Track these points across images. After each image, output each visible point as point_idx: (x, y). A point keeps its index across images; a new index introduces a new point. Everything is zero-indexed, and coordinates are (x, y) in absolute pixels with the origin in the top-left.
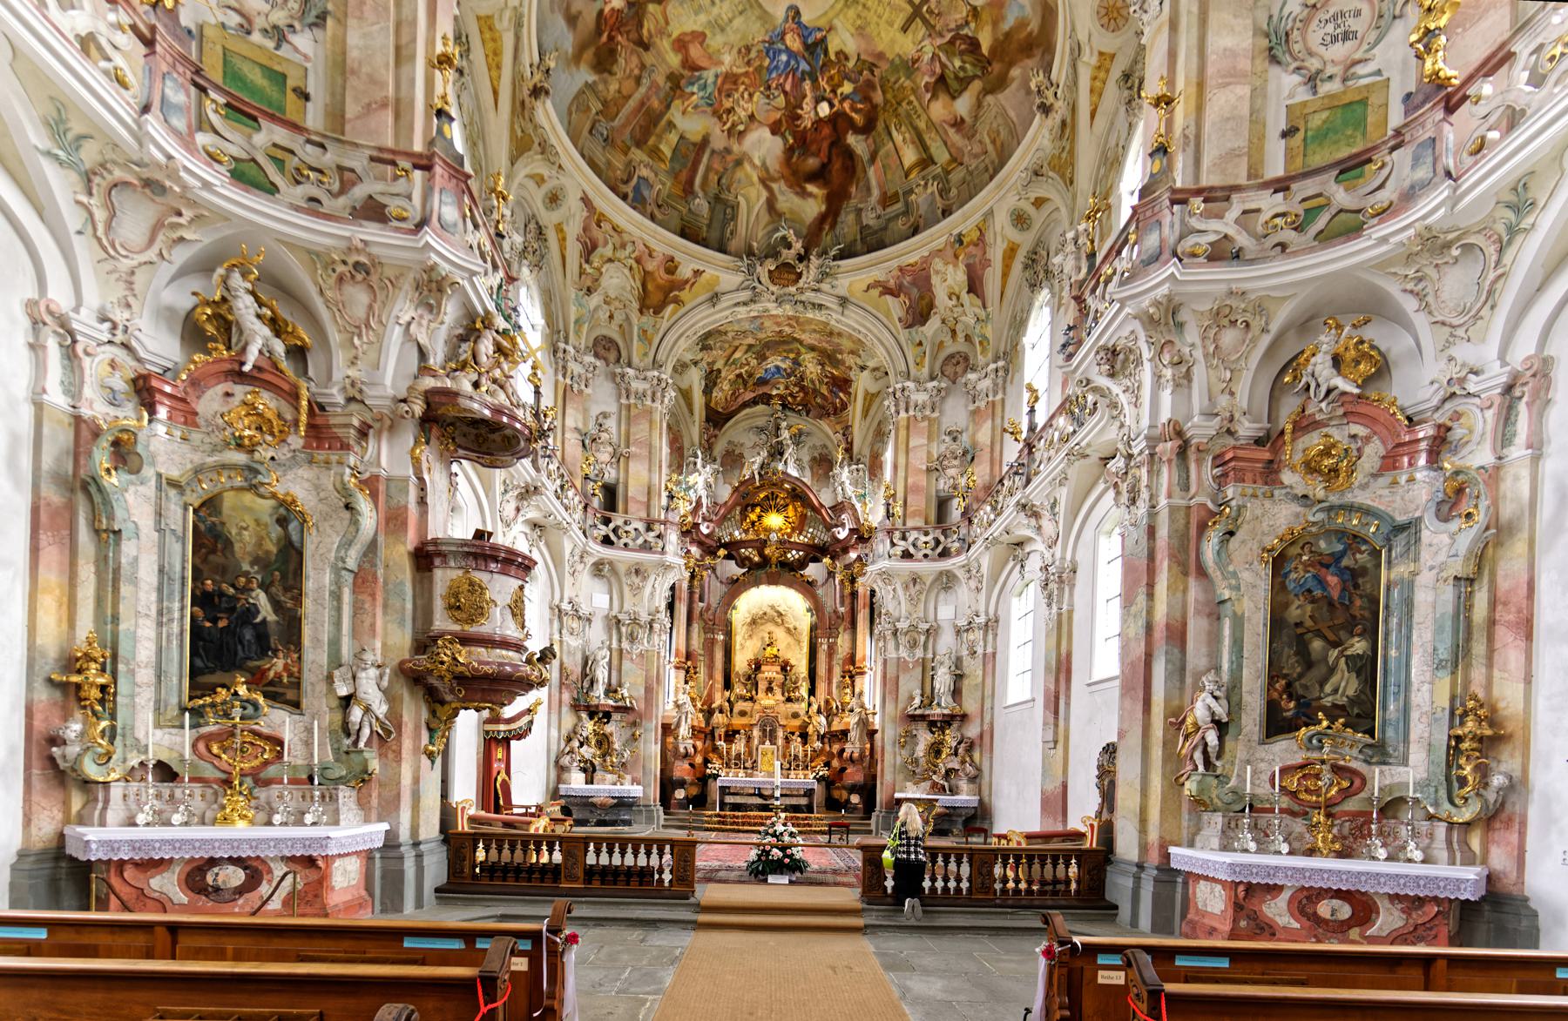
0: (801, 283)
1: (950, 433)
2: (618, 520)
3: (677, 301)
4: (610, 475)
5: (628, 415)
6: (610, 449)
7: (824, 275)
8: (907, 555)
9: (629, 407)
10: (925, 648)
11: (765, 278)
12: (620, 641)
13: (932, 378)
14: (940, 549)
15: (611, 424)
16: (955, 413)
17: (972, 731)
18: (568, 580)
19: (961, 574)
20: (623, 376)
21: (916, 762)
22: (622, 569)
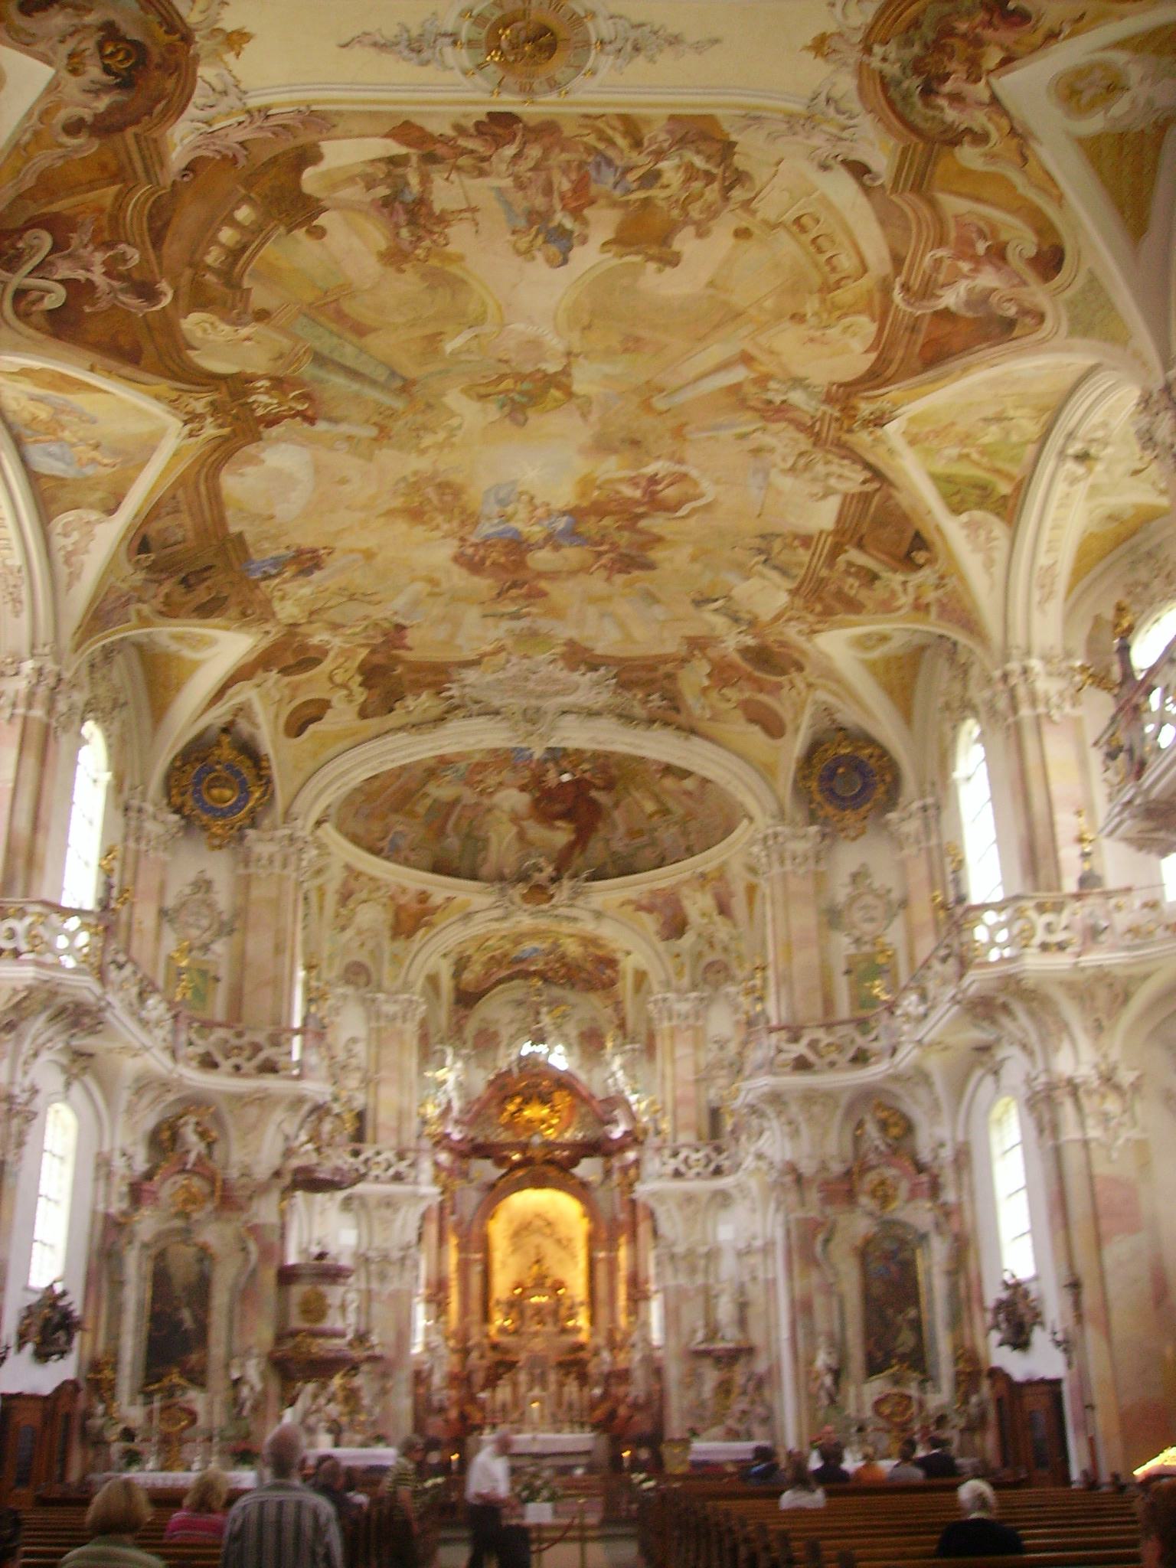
0: (554, 901)
1: (716, 1042)
2: (368, 1152)
3: (430, 925)
4: (360, 1101)
5: (378, 1038)
6: (358, 1075)
7: (576, 894)
8: (677, 1174)
9: (379, 1030)
10: (706, 1272)
11: (517, 899)
12: (368, 1281)
13: (694, 987)
14: (712, 1167)
15: (360, 1048)
16: (721, 1022)
17: (761, 1366)
18: (317, 1219)
19: (734, 1192)
20: (373, 1000)
21: (702, 1405)
22: (372, 1202)
